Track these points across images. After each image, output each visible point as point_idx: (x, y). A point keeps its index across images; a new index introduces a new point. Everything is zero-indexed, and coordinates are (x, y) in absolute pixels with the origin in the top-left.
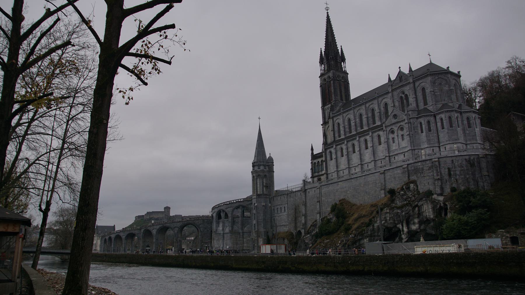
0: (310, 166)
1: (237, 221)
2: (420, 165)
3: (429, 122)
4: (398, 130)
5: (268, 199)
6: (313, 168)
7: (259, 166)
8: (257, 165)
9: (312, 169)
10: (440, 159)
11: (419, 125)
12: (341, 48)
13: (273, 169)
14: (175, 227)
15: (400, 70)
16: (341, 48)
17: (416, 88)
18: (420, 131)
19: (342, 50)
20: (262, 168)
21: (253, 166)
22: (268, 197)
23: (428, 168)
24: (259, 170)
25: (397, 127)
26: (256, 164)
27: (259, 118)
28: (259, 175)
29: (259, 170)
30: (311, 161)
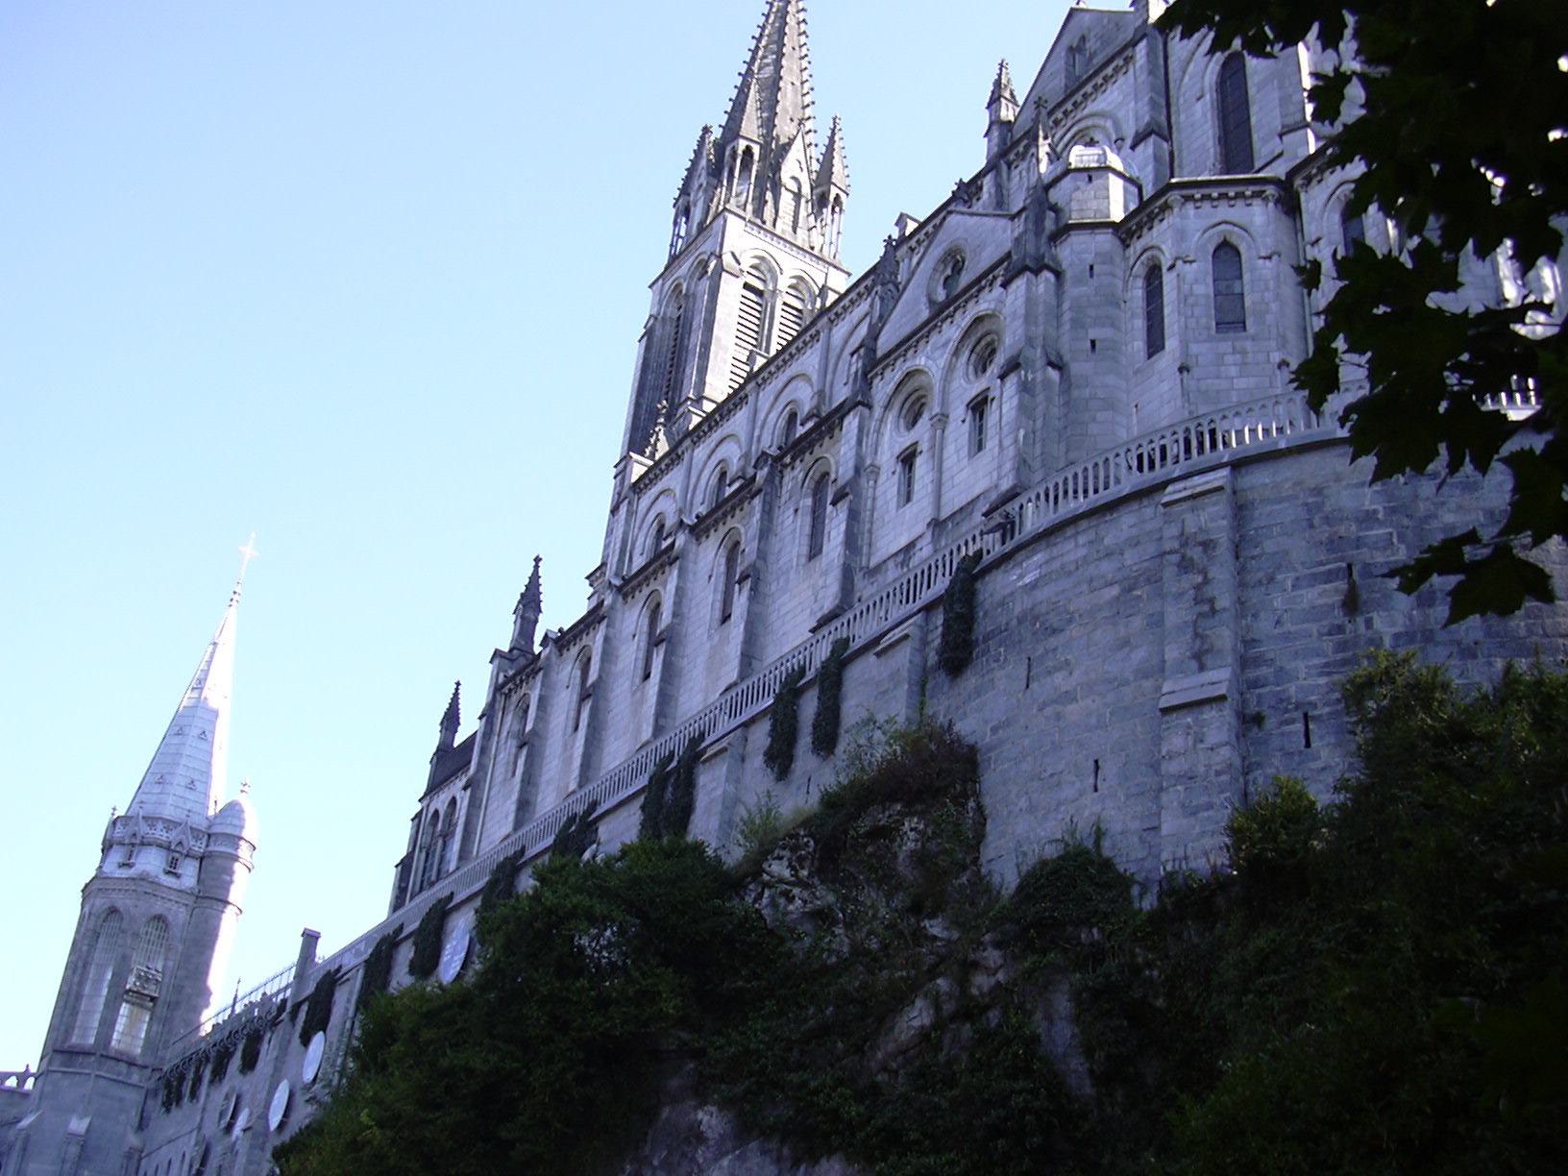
2: (1033, 586)
3: (1226, 253)
4: (950, 369)
6: (419, 858)
9: (405, 866)
10: (1259, 478)
11: (1137, 292)
17: (1173, 76)
18: (1139, 345)
20: (151, 862)
21: (107, 847)
22: (135, 1078)
23: (1115, 591)
24: (125, 873)
25: (951, 346)
28: (113, 911)
29: (125, 873)
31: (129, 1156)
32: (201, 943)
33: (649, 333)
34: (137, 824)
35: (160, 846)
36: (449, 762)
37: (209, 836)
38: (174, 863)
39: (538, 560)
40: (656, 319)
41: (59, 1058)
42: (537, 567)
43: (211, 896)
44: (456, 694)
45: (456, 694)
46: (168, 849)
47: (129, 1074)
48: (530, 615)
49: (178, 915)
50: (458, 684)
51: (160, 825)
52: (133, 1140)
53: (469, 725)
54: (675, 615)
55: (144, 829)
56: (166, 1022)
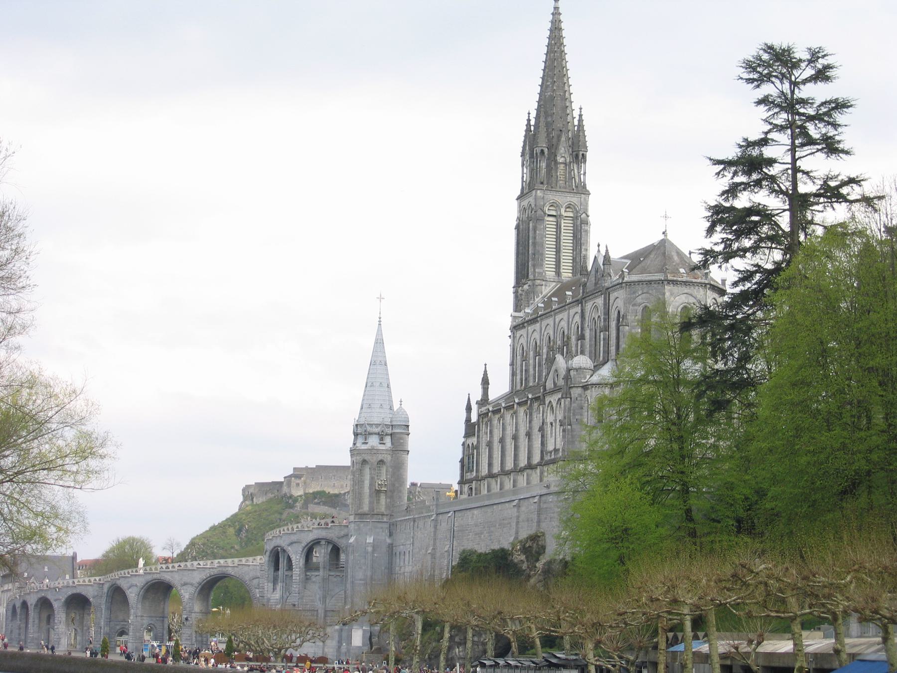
0: (459, 454)
1: (314, 579)
5: (387, 526)
7: (367, 435)
8: (361, 434)
9: (462, 461)
12: (580, 116)
13: (403, 444)
14: (185, 584)
15: (599, 251)
16: (580, 116)
19: (581, 120)
20: (374, 441)
21: (356, 435)
22: (385, 520)
26: (359, 430)
27: (381, 298)
30: (463, 440)
31: (389, 547)
32: (398, 469)
33: (517, 227)
34: (365, 427)
35: (376, 434)
36: (471, 429)
37: (392, 425)
38: (382, 439)
39: (486, 365)
40: (519, 220)
41: (357, 517)
42: (486, 367)
43: (399, 449)
44: (469, 398)
45: (469, 398)
46: (379, 434)
47: (383, 519)
48: (486, 386)
49: (388, 458)
50: (469, 394)
51: (374, 426)
52: (389, 541)
53: (474, 418)
54: (516, 431)
55: (369, 429)
56: (391, 497)
